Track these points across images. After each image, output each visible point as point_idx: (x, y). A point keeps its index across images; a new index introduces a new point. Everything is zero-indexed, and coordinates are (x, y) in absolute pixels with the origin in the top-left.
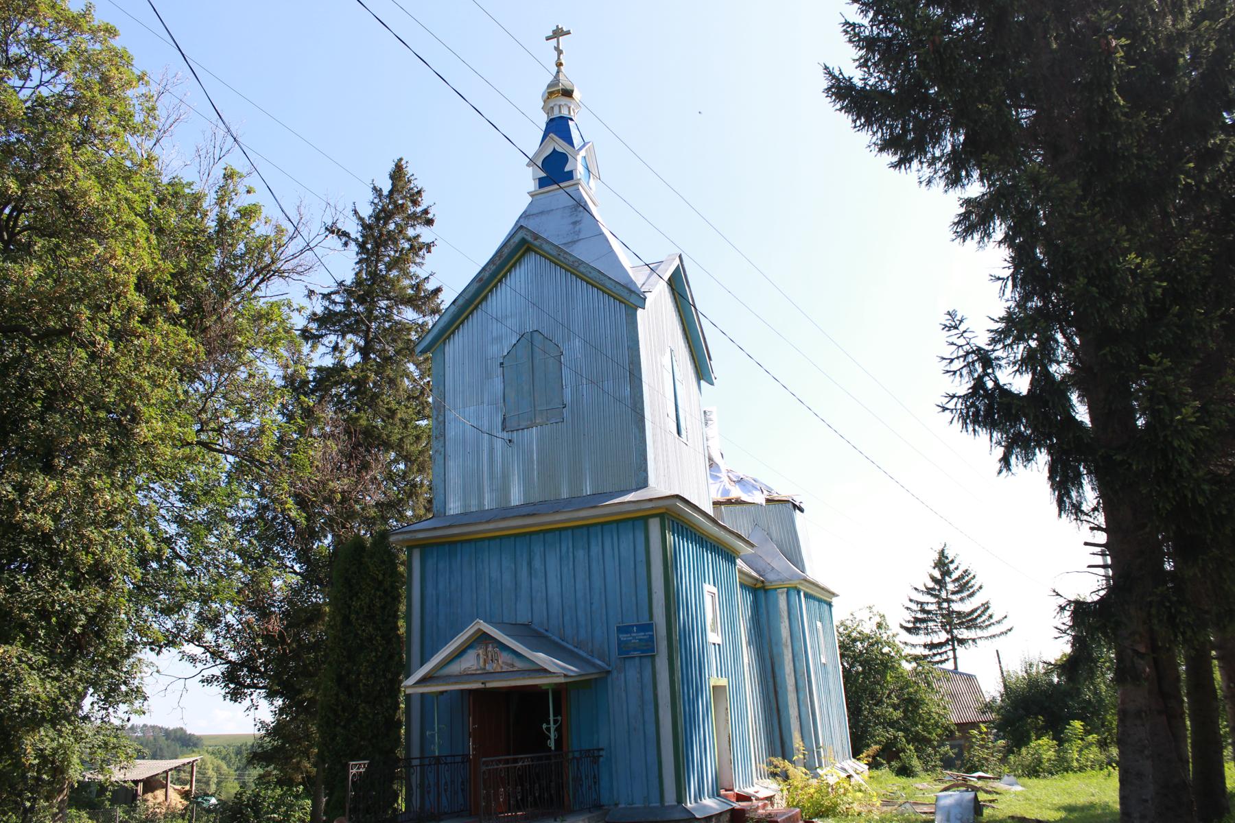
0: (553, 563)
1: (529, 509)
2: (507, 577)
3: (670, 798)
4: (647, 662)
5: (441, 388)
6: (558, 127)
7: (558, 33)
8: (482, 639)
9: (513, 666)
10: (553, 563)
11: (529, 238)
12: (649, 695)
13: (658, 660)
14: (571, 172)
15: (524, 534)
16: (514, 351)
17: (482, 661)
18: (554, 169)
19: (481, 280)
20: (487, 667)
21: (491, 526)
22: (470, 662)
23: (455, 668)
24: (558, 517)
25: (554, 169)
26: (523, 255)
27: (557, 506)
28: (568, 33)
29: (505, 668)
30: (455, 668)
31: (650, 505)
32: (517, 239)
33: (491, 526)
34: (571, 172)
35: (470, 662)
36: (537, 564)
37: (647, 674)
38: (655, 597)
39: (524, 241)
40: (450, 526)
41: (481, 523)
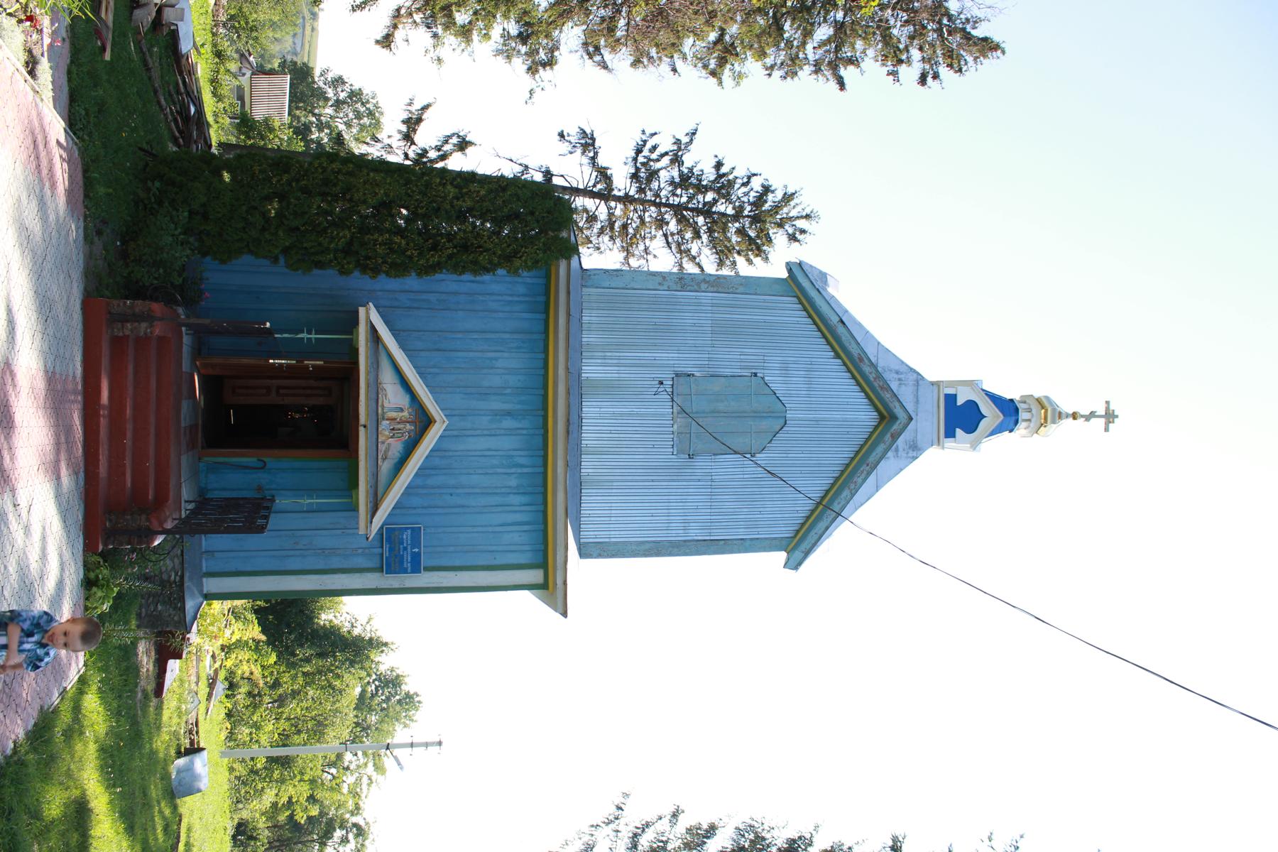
0: (507, 443)
1: (574, 376)
2: (496, 381)
3: (211, 585)
4: (374, 563)
5: (741, 289)
6: (1010, 411)
7: (1110, 416)
8: (424, 421)
9: (384, 459)
10: (507, 443)
11: (896, 427)
12: (336, 563)
13: (377, 575)
14: (954, 436)
15: (545, 409)
16: (767, 391)
17: (393, 414)
18: (962, 417)
19: (861, 360)
20: (385, 423)
21: (561, 371)
22: (393, 398)
23: (387, 377)
24: (560, 463)
25: (962, 417)
26: (877, 410)
27: (574, 465)
28: (1106, 430)
29: (382, 448)
30: (387, 377)
31: (559, 582)
32: (898, 411)
33: (561, 371)
34: (954, 436)
35: (393, 398)
36: (508, 423)
37: (361, 562)
38: (451, 574)
39: (894, 418)
40: (568, 314)
41: (567, 360)
